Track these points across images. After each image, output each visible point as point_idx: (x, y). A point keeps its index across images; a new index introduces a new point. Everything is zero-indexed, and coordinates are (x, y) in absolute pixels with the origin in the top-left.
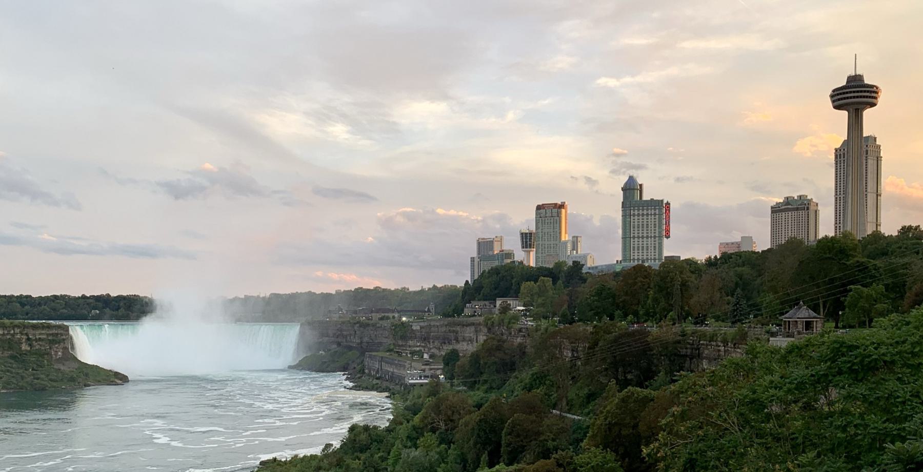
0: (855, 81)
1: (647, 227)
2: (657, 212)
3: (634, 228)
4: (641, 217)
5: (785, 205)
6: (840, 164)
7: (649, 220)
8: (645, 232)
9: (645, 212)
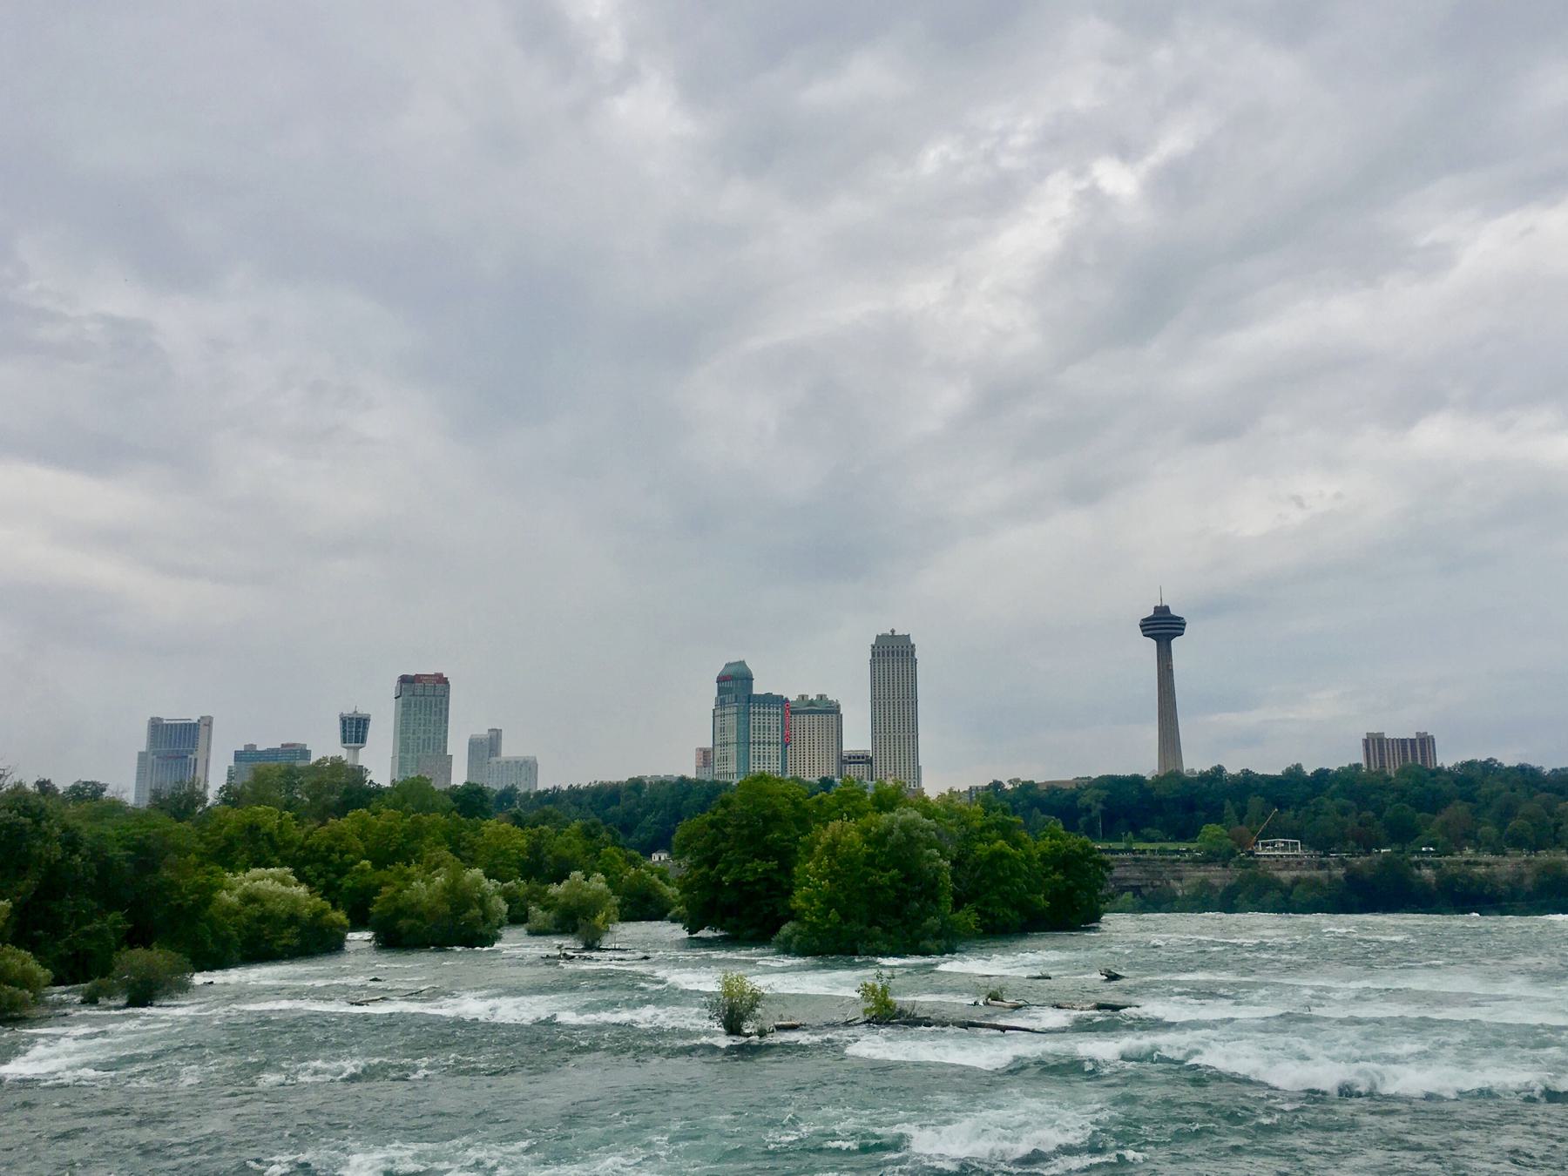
0: (1162, 613)
1: (769, 730)
2: (780, 711)
3: (754, 730)
4: (762, 717)
5: (808, 706)
6: (903, 662)
7: (771, 721)
8: (767, 736)
9: (767, 710)
